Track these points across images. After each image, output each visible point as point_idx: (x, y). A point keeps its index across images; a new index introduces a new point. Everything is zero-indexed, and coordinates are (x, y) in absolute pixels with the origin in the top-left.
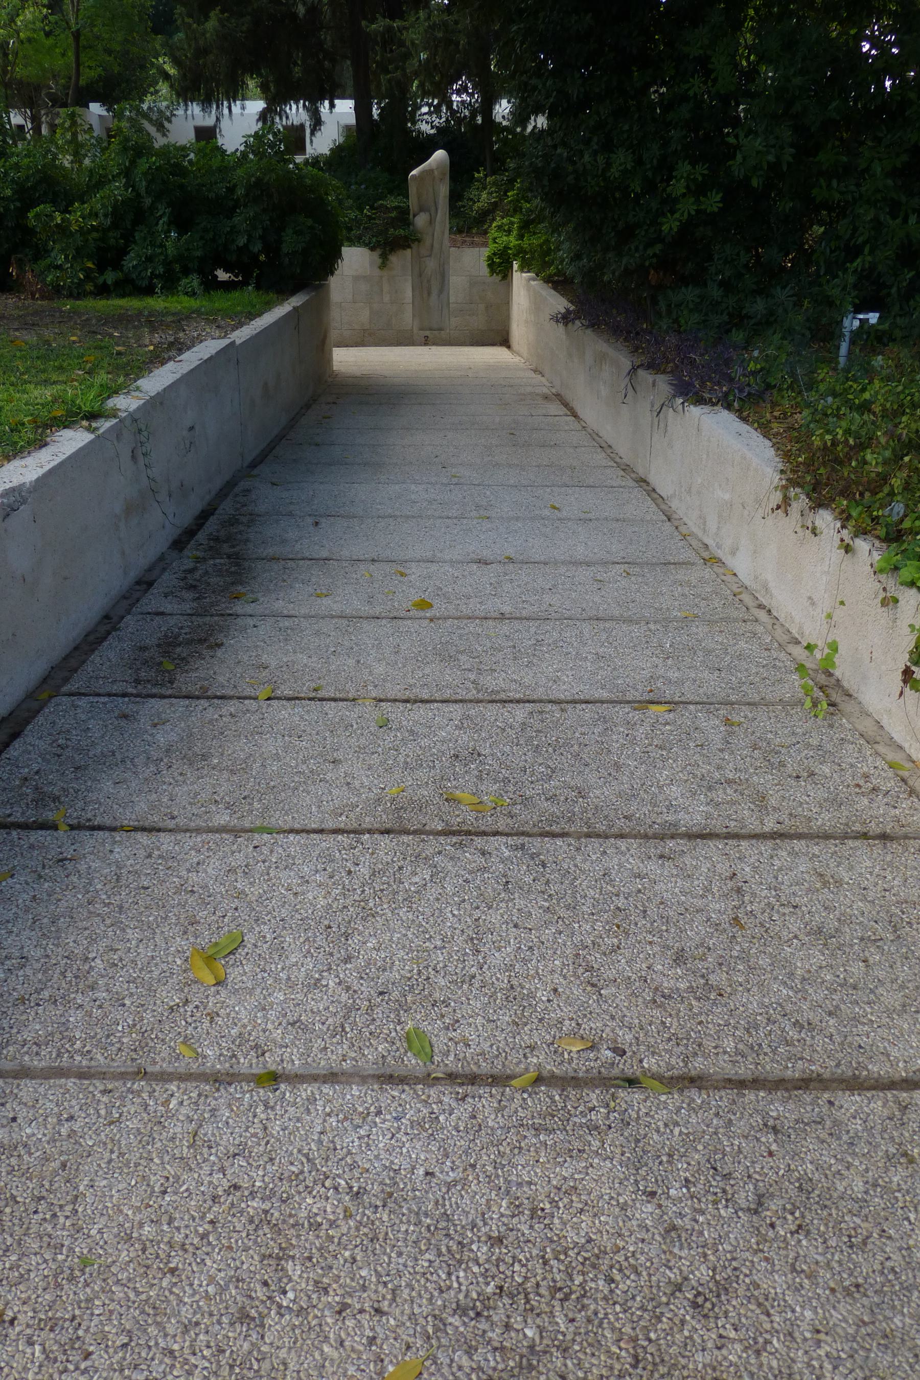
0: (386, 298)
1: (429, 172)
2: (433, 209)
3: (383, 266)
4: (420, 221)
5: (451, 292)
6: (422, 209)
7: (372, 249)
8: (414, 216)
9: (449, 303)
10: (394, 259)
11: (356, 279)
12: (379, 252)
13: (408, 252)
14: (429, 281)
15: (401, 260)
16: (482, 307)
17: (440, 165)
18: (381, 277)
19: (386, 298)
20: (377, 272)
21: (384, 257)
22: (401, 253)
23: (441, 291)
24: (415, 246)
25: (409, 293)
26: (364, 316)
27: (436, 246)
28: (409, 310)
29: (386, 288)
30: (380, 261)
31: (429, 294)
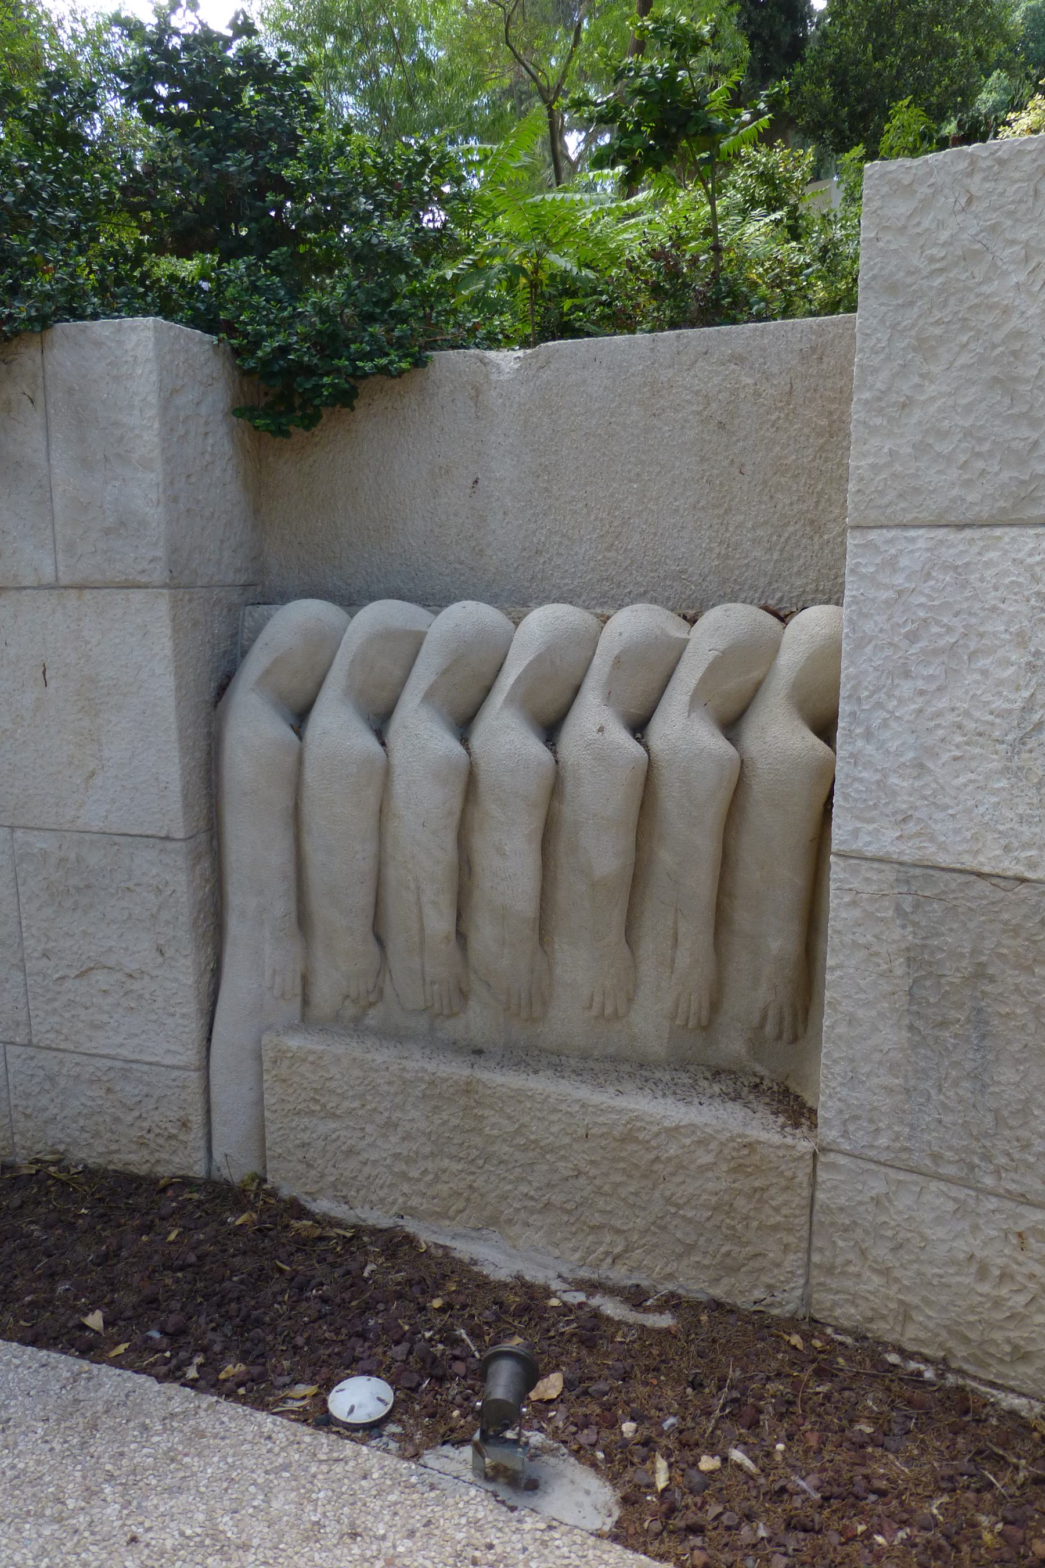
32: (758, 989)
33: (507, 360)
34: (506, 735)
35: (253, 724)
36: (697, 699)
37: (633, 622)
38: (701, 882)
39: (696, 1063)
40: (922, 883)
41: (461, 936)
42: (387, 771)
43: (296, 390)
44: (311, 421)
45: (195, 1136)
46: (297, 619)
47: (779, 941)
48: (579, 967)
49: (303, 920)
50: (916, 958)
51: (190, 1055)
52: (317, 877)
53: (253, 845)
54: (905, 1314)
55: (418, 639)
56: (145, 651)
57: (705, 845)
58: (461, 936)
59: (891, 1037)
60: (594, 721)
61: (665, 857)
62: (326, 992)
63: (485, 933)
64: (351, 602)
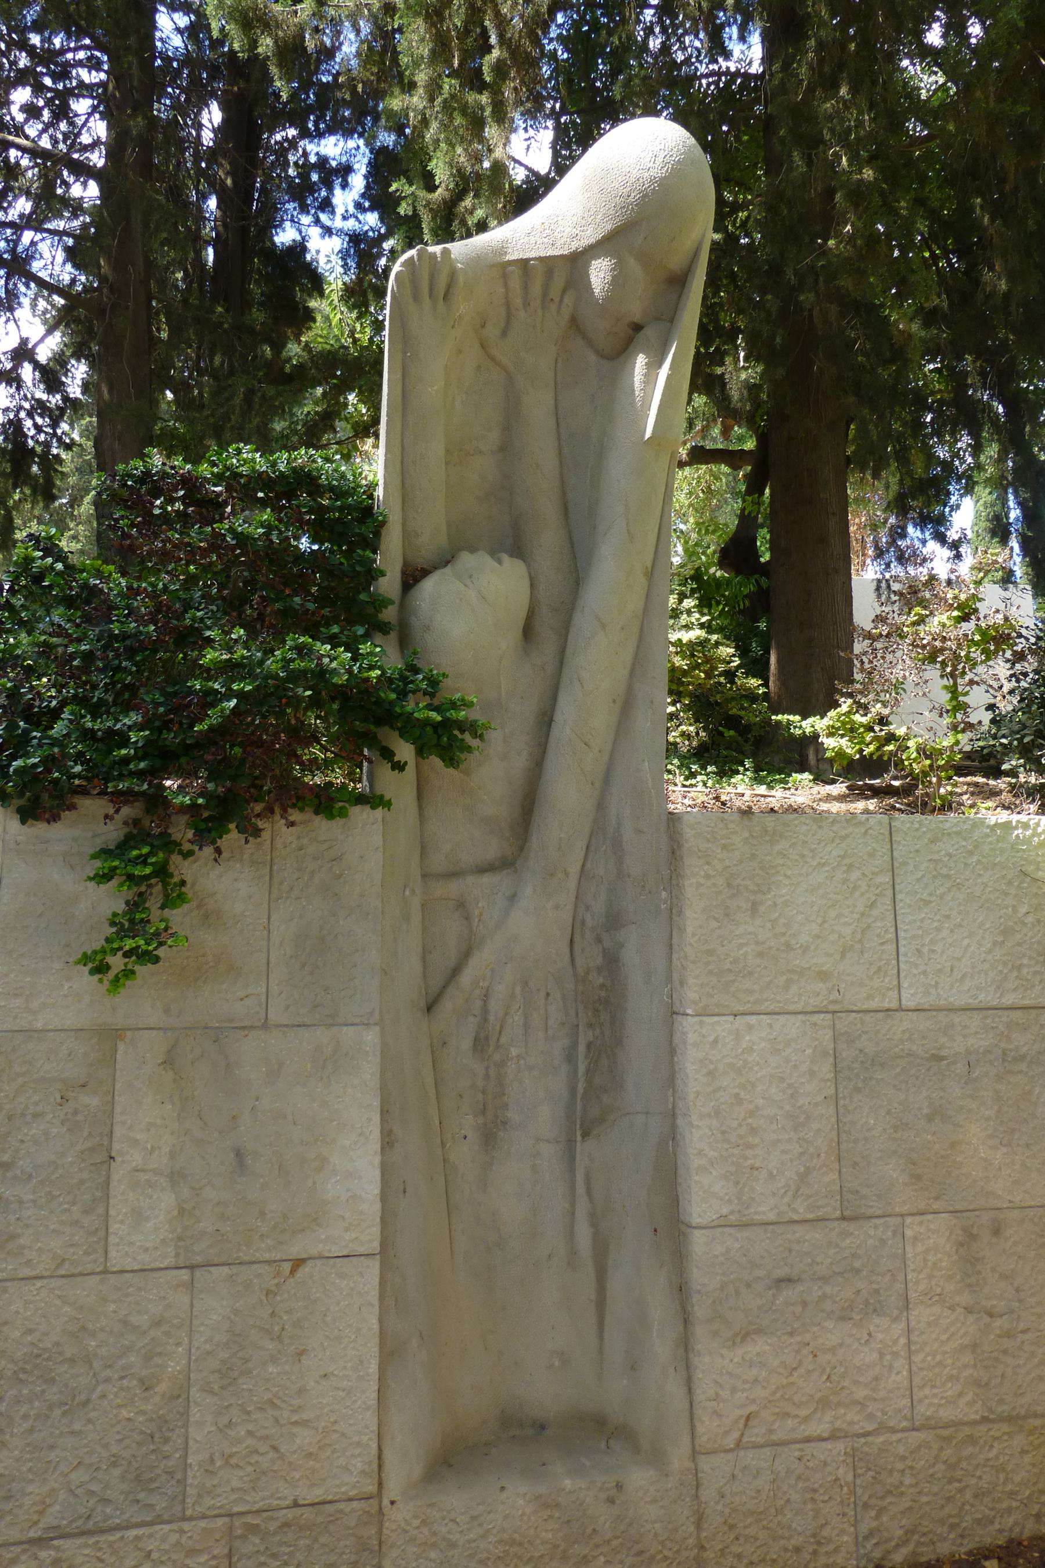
0: (143, 1226)
2: (548, 540)
3: (131, 946)
4: (467, 618)
8: (413, 577)
9: (672, 1231)
10: (230, 884)
12: (91, 825)
16: (931, 1241)
18: (109, 1037)
19: (143, 1226)
21: (144, 868)
22: (291, 837)
25: (354, 1174)
27: (567, 793)
28: (350, 1309)
29: (145, 1125)
30: (109, 900)
31: (491, 1134)
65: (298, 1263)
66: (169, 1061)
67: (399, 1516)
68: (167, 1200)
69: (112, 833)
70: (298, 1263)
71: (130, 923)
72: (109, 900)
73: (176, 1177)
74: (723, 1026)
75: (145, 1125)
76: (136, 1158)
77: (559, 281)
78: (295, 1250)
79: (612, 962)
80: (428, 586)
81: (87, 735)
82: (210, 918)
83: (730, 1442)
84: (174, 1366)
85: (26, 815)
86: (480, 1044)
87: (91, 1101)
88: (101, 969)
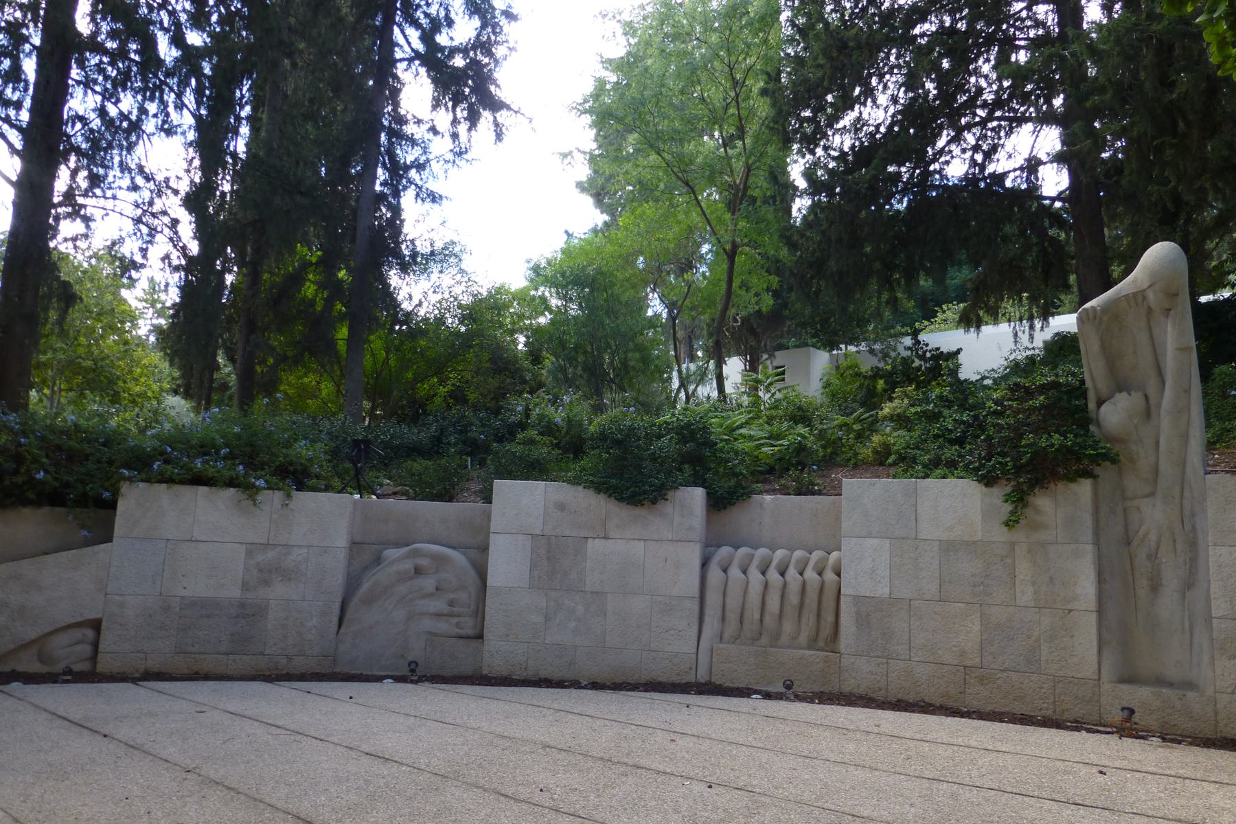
0: (1025, 595)
1: (1138, 297)
5: (1215, 588)
6: (1121, 386)
7: (989, 481)
9: (1209, 619)
10: (1043, 502)
11: (949, 547)
13: (1084, 488)
14: (1153, 556)
15: (1066, 506)
17: (1157, 276)
18: (1013, 544)
20: (1001, 534)
21: (1019, 499)
23: (1189, 583)
24: (1105, 472)
25: (1087, 588)
26: (969, 634)
28: (1087, 626)
29: (1024, 569)
30: (1008, 507)
32: (826, 631)
33: (768, 498)
34: (773, 575)
35: (715, 574)
36: (814, 568)
37: (798, 554)
38: (814, 605)
39: (812, 644)
40: (858, 599)
41: (761, 621)
42: (748, 583)
43: (718, 503)
44: (725, 508)
45: (693, 672)
46: (725, 551)
47: (830, 618)
48: (788, 627)
49: (723, 619)
50: (858, 613)
51: (694, 650)
52: (728, 607)
53: (713, 599)
54: (859, 686)
55: (753, 555)
56: (693, 554)
57: (815, 597)
58: (761, 621)
59: (854, 629)
60: (792, 572)
61: (807, 601)
62: (727, 635)
63: (767, 619)
64: (737, 547)
65: (1070, 611)
66: (1029, 551)
67: (1106, 687)
68: (1031, 589)
69: (1009, 489)
70: (1070, 611)
71: (1012, 513)
72: (1008, 507)
73: (1034, 583)
74: (1224, 550)
75: (1024, 569)
76: (1021, 577)
77: (1140, 299)
78: (1070, 607)
79: (1194, 528)
80: (1103, 408)
81: (1000, 463)
82: (1037, 511)
83: (1230, 690)
84: (1036, 633)
85: (987, 485)
86: (1149, 557)
87: (1009, 561)
88: (1007, 524)
